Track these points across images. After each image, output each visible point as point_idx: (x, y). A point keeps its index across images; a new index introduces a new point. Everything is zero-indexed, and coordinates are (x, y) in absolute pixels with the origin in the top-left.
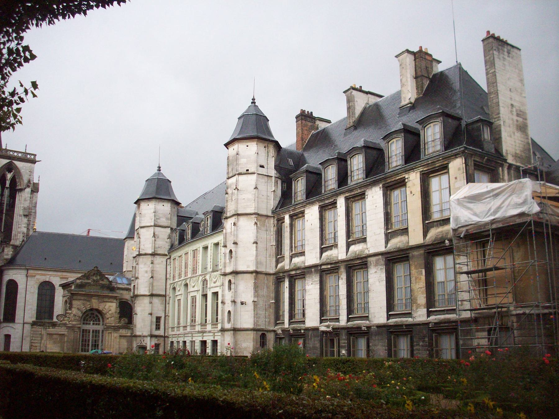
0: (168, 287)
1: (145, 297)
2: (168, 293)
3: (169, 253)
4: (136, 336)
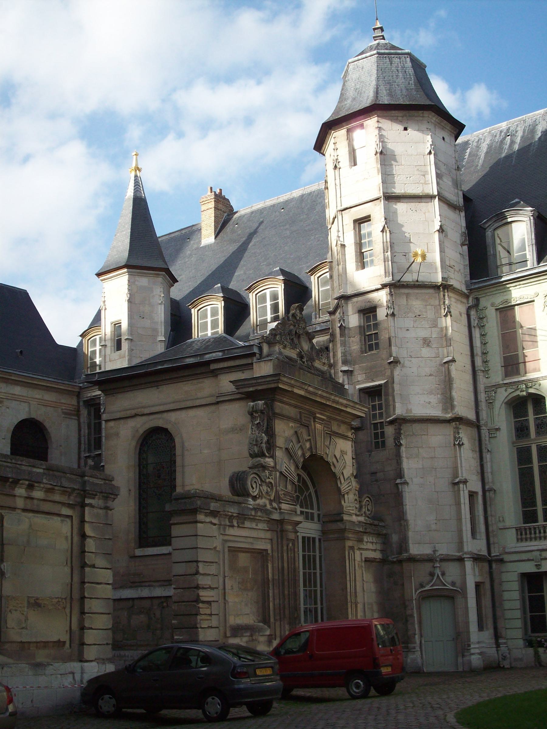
0: (482, 397)
1: (433, 429)
2: (484, 415)
3: (471, 291)
4: (413, 559)
